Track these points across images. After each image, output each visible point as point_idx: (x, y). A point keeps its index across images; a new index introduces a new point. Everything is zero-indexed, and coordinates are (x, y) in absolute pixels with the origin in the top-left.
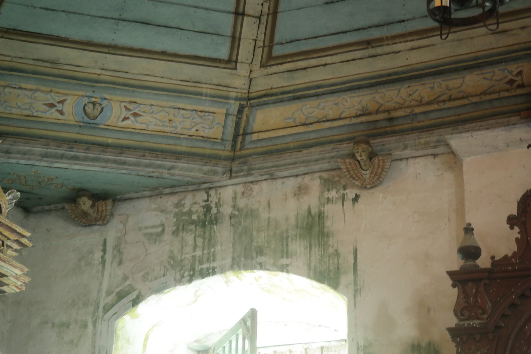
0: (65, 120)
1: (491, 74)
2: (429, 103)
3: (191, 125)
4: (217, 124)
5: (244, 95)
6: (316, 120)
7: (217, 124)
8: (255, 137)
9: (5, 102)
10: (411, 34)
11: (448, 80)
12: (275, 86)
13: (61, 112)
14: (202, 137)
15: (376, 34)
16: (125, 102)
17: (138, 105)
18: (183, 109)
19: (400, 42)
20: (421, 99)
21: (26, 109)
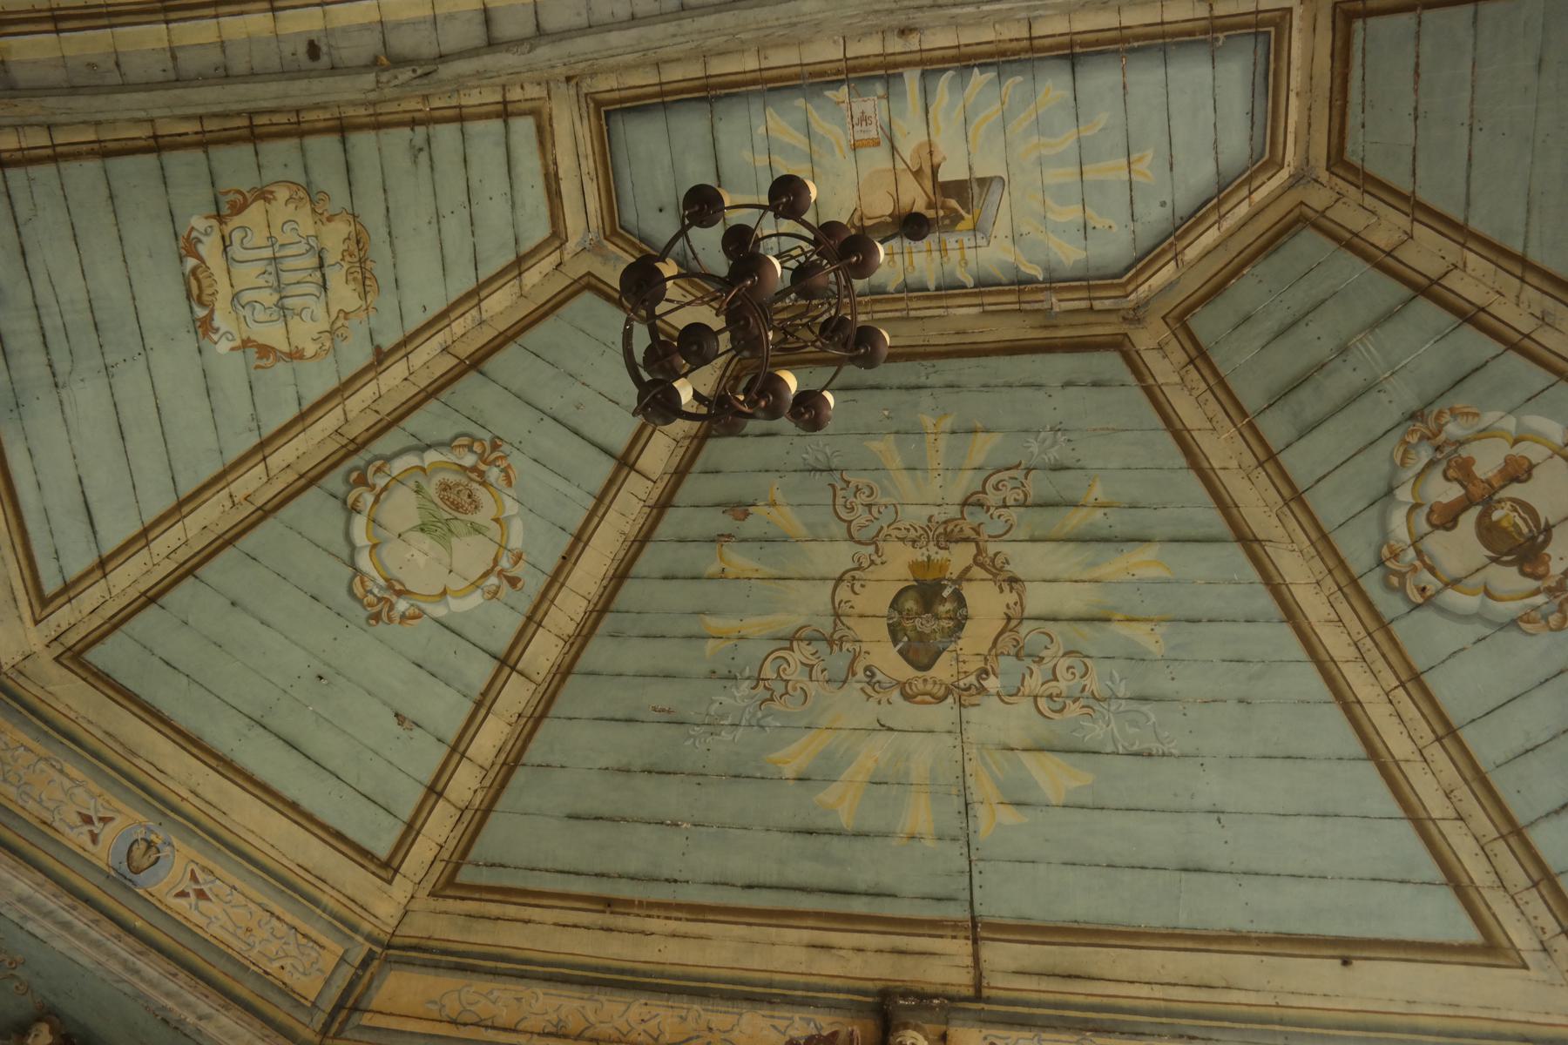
0: (93, 854)
1: (786, 1023)
3: (277, 953)
4: (318, 970)
5: (382, 936)
6: (475, 1019)
7: (318, 970)
8: (366, 1020)
9: (26, 783)
10: (679, 907)
11: (713, 1011)
12: (437, 937)
13: (94, 838)
14: (284, 983)
15: (625, 890)
16: (197, 864)
17: (213, 878)
18: (278, 918)
19: (658, 917)
20: (659, 1036)
21: (48, 809)
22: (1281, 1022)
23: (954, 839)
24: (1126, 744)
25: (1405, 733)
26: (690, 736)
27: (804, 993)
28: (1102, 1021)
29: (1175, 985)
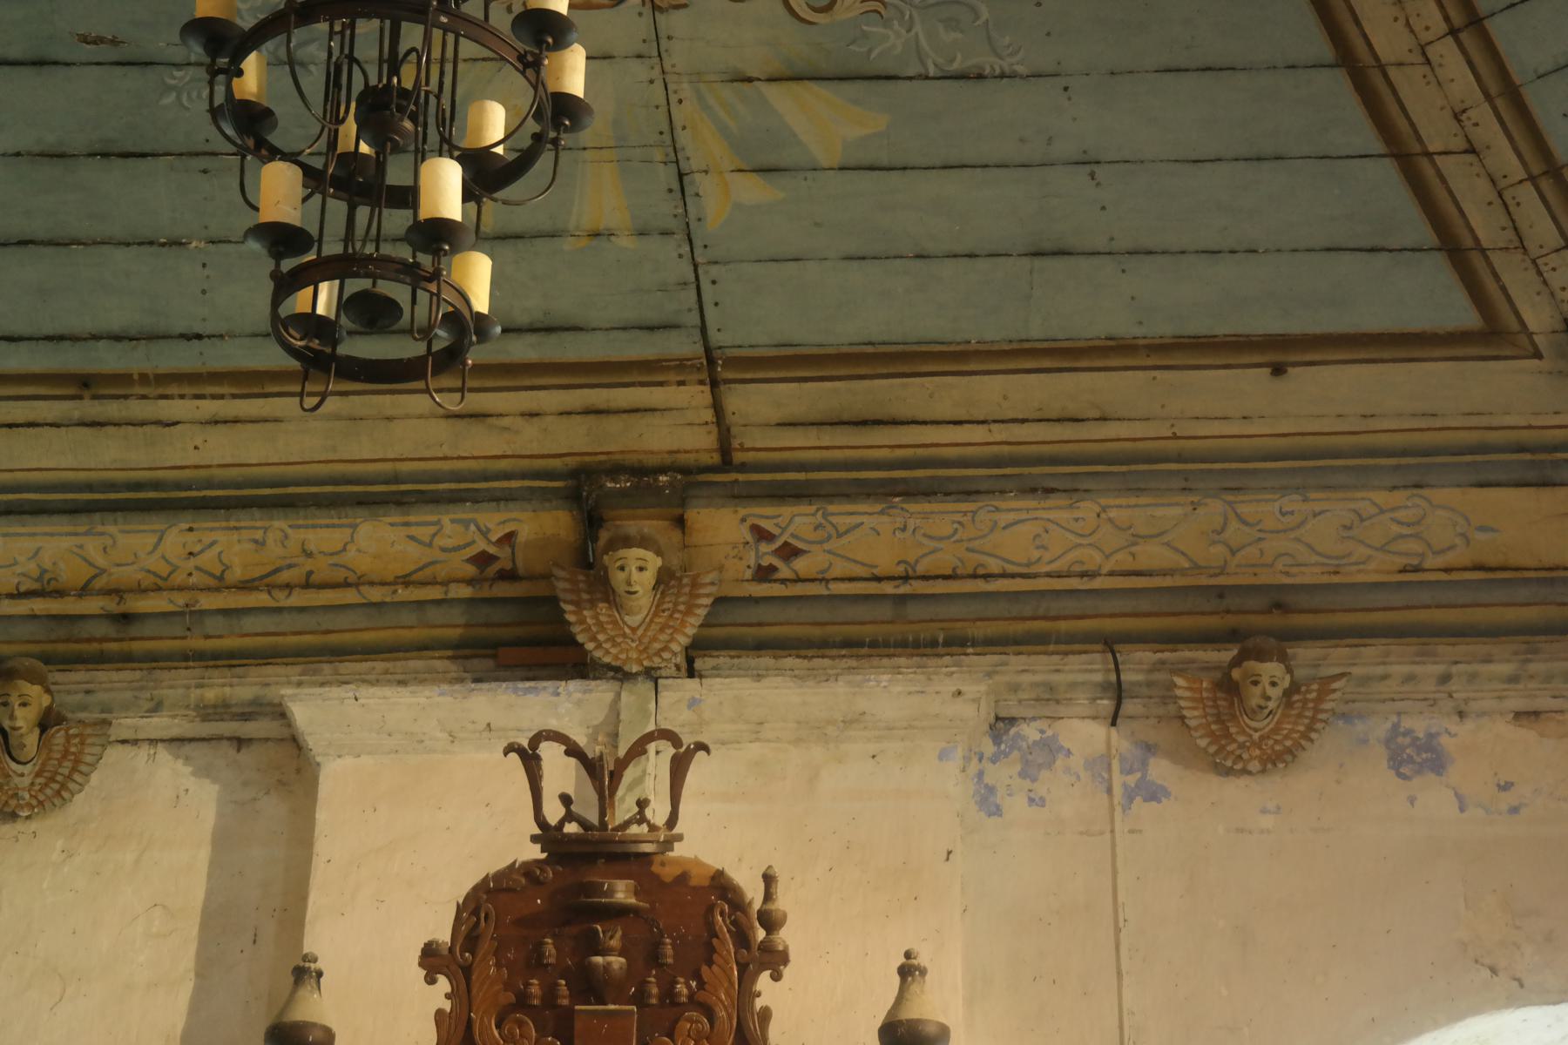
1: (432, 529)
2: (246, 586)
11: (306, 527)
15: (108, 359)
19: (182, 397)
20: (223, 571)
22: (1180, 458)
23: (666, 233)
24: (940, 61)
25: (1402, 21)
26: (170, 89)
27: (453, 486)
28: (916, 480)
29: (1023, 421)
